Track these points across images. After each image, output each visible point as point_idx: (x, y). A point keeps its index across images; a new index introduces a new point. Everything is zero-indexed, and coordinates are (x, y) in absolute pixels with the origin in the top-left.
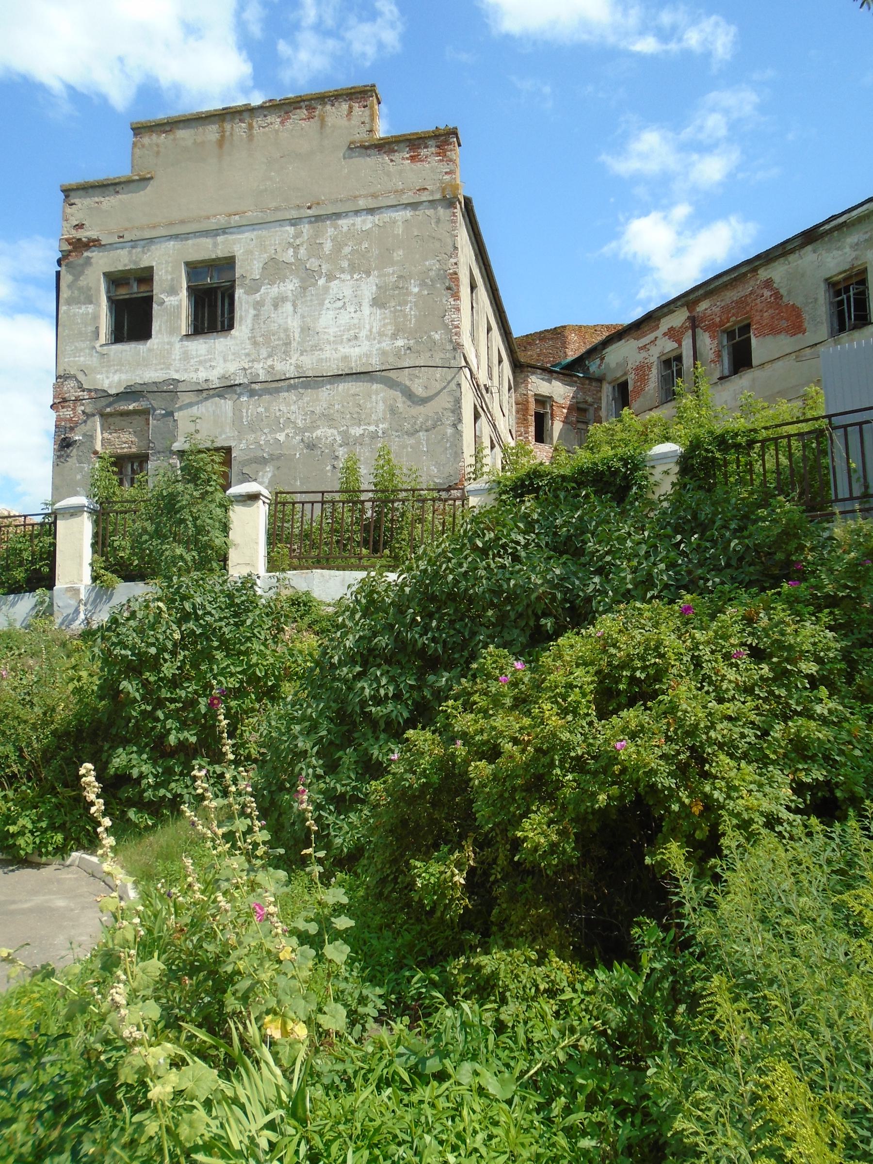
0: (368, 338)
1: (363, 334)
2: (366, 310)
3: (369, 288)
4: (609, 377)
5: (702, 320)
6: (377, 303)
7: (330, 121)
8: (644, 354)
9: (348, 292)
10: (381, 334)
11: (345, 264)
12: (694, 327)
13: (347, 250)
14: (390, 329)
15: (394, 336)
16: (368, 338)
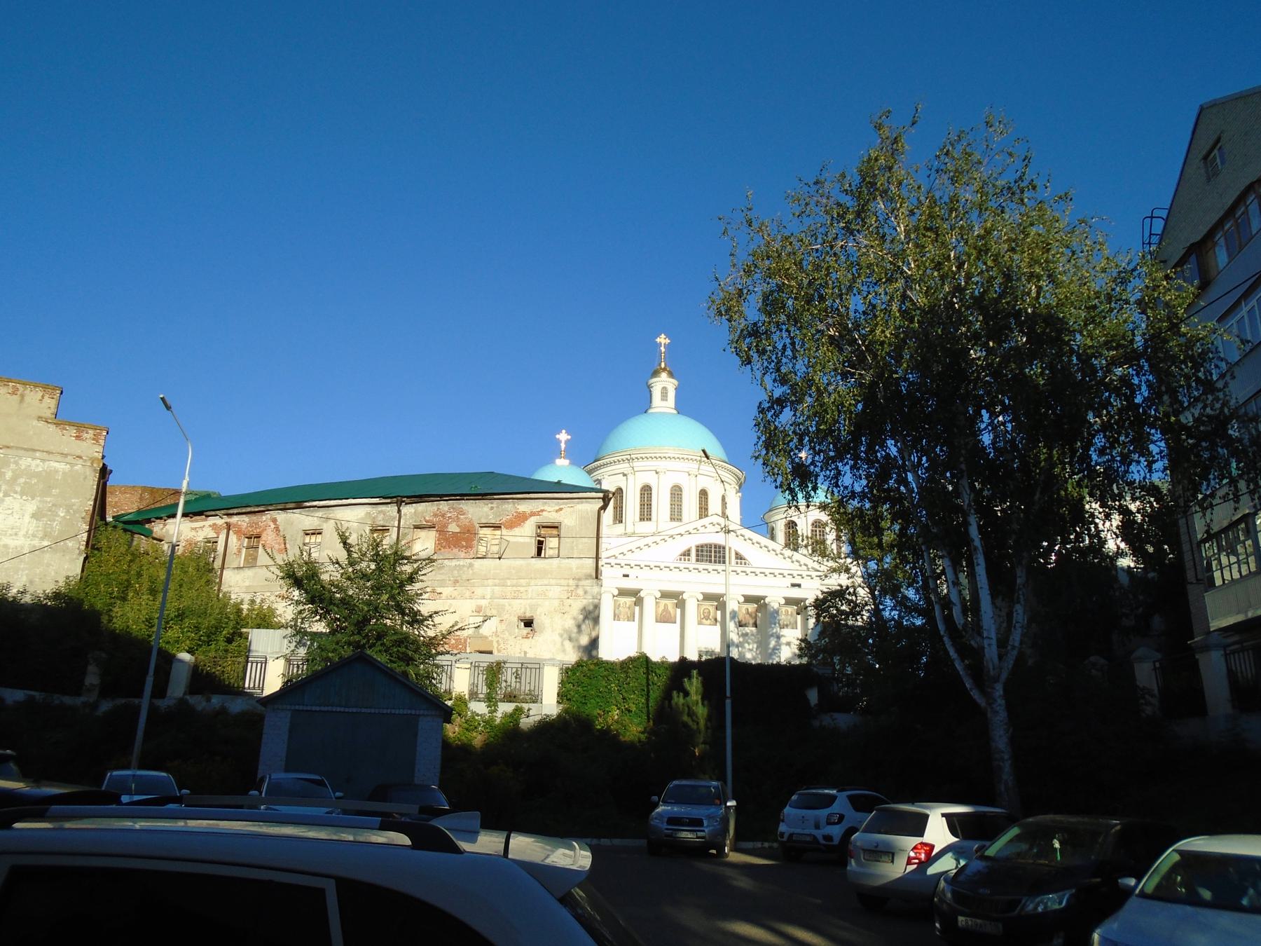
0: (25, 536)
1: (23, 532)
2: (27, 518)
3: (31, 507)
4: (166, 540)
5: (236, 525)
6: (34, 516)
7: (27, 399)
8: (194, 533)
9: (16, 506)
10: (34, 536)
11: (18, 489)
12: (229, 530)
13: (22, 480)
14: (41, 534)
15: (42, 539)
16: (25, 536)
